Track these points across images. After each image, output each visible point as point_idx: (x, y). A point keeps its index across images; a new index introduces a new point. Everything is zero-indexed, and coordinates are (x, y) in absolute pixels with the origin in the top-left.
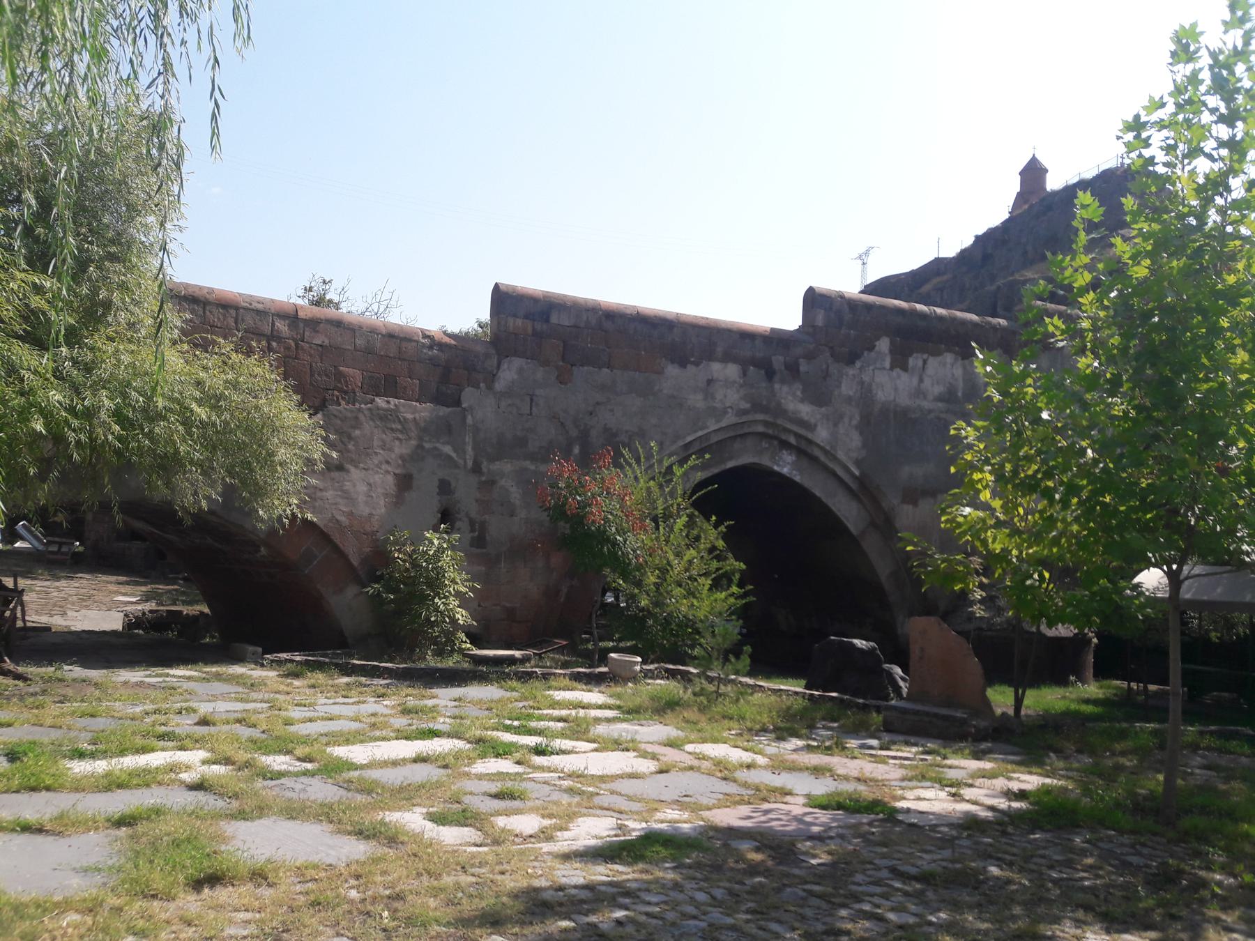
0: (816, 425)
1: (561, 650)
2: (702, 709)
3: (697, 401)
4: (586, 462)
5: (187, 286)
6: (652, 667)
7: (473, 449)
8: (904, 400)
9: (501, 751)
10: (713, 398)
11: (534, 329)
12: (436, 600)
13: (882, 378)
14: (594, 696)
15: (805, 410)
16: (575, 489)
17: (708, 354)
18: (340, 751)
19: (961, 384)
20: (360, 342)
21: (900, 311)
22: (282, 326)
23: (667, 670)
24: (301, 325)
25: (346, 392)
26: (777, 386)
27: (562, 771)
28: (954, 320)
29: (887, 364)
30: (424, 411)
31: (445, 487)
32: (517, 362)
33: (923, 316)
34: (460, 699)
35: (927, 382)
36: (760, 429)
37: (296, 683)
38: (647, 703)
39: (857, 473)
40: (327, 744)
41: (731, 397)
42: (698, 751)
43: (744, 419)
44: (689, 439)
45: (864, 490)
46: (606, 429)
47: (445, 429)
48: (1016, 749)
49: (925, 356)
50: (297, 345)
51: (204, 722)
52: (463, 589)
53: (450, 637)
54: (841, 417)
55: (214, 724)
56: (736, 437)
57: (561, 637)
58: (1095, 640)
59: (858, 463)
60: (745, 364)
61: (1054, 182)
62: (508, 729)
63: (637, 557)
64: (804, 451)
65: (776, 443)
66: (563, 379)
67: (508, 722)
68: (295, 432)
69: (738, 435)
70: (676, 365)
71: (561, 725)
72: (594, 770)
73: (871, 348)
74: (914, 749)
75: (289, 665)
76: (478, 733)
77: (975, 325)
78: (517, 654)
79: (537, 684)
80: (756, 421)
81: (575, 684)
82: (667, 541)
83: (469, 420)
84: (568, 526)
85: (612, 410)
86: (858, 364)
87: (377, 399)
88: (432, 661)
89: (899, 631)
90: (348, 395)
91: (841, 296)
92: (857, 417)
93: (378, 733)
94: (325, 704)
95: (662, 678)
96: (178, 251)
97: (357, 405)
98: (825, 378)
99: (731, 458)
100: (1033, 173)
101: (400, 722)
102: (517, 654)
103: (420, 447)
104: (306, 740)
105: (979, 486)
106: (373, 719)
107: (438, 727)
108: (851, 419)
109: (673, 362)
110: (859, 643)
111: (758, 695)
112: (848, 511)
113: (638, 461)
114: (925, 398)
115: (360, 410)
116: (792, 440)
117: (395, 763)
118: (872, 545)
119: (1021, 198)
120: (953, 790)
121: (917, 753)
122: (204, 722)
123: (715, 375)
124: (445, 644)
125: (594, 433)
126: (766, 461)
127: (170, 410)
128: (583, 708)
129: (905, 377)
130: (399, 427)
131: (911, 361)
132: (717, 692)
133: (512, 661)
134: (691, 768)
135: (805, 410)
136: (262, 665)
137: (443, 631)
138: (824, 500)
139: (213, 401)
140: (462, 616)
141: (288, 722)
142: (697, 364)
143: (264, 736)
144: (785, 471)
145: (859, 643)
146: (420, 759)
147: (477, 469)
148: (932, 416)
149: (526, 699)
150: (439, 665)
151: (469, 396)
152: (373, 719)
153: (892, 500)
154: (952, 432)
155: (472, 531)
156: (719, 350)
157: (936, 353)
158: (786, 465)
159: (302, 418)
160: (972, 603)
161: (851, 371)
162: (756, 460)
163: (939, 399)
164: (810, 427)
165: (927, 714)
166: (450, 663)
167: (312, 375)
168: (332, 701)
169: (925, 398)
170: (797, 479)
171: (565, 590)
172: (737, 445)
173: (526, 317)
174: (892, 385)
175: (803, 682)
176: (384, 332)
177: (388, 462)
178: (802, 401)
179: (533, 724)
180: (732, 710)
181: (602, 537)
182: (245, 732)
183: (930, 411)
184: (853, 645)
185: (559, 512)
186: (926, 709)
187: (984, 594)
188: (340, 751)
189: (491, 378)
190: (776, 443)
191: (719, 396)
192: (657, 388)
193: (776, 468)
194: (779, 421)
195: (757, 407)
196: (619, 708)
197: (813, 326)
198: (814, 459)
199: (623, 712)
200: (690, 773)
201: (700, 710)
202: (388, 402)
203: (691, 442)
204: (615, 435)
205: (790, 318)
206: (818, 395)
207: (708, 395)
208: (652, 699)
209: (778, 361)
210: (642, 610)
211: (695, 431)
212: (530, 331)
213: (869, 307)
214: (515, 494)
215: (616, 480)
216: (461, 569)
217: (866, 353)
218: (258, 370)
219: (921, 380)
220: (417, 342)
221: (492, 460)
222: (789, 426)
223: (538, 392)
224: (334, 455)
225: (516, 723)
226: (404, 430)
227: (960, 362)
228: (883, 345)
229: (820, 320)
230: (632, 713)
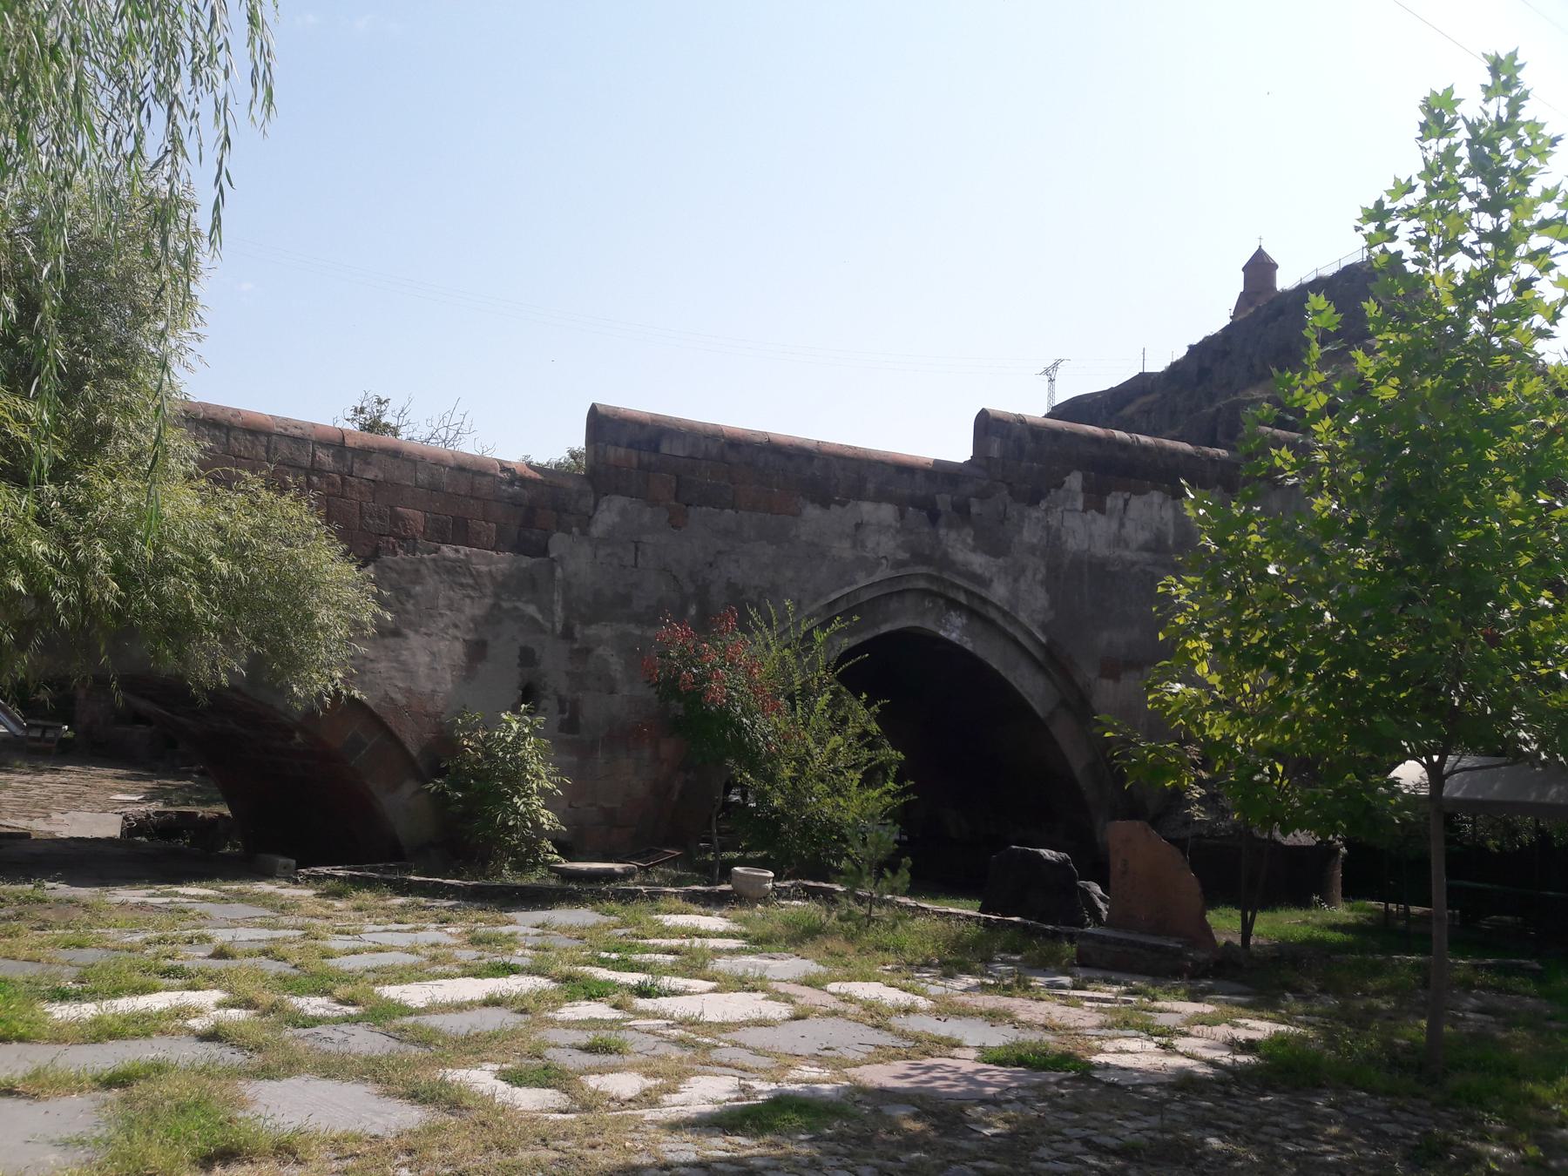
0: (991, 581)
1: (672, 863)
2: (850, 938)
3: (843, 549)
4: (705, 625)
5: (206, 406)
6: (787, 884)
7: (563, 608)
8: (1101, 550)
9: (596, 992)
10: (863, 546)
11: (639, 460)
12: (516, 800)
13: (1073, 522)
14: (713, 922)
15: (978, 562)
16: (691, 659)
17: (857, 491)
18: (392, 992)
19: (1171, 529)
20: (422, 477)
21: (1095, 440)
22: (324, 456)
23: (806, 888)
24: (349, 455)
25: (404, 539)
26: (942, 532)
27: (671, 1017)
28: (1162, 449)
30: (501, 562)
31: (527, 657)
32: (619, 501)
33: (1123, 445)
34: (544, 926)
35: (1129, 528)
36: (922, 584)
37: (338, 904)
38: (780, 930)
39: (1043, 640)
40: (375, 983)
41: (886, 545)
42: (843, 991)
43: (902, 572)
44: (834, 596)
45: (1052, 661)
47: (528, 584)
48: (1240, 987)
49: (1127, 495)
50: (343, 480)
51: (221, 954)
52: (549, 785)
53: (533, 847)
54: (1023, 570)
55: (233, 957)
56: (892, 594)
57: (673, 846)
58: (1343, 850)
59: (1044, 628)
60: (902, 504)
61: (1285, 280)
62: (604, 963)
63: (768, 744)
64: (977, 612)
65: (941, 602)
66: (676, 522)
67: (604, 955)
68: (339, 587)
69: (895, 592)
71: (671, 958)
72: (711, 1016)
73: (1060, 485)
74: (1115, 989)
75: (329, 882)
76: (566, 969)
77: (1188, 456)
78: (618, 867)
79: (642, 906)
80: (916, 575)
81: (691, 906)
82: (806, 724)
83: (559, 572)
84: (681, 705)
86: (1043, 505)
87: (444, 548)
88: (509, 877)
90: (408, 542)
91: (1021, 420)
92: (1043, 570)
93: (439, 969)
94: (373, 933)
95: (799, 899)
96: (195, 364)
97: (418, 555)
98: (1002, 522)
99: (885, 621)
100: (1259, 269)
101: (468, 955)
102: (618, 867)
103: (496, 606)
104: (349, 978)
105: (1195, 657)
106: (434, 951)
107: (515, 961)
109: (813, 501)
110: (1046, 853)
111: (919, 920)
112: (1032, 687)
113: (769, 625)
114: (1127, 546)
115: (421, 561)
116: (962, 598)
117: (460, 1007)
118: (1063, 732)
119: (1245, 299)
120: (1164, 1040)
121: (1119, 993)
122: (221, 954)
123: (866, 518)
124: (527, 855)
126: (929, 625)
127: (182, 562)
128: (700, 936)
129: (1102, 520)
130: (471, 581)
131: (1109, 502)
132: (868, 916)
133: (610, 876)
134: (835, 1013)
135: (978, 562)
136: (296, 882)
137: (523, 839)
139: (236, 551)
140: (547, 819)
141: (327, 955)
142: (842, 504)
143: (296, 972)
144: (954, 636)
145: (1046, 853)
146: (492, 1002)
147: (568, 634)
148: (1136, 569)
149: (627, 925)
150: (518, 882)
151: (559, 544)
152: (434, 951)
154: (1160, 590)
155: (562, 711)
156: (871, 487)
157: (1140, 492)
158: (954, 630)
159: (350, 571)
160: (1190, 803)
162: (917, 623)
163: (1145, 547)
164: (985, 583)
165: (1133, 943)
166: (532, 879)
167: (362, 518)
168: (382, 928)
169: (1127, 546)
170: (969, 647)
172: (894, 605)
173: (630, 446)
174: (1086, 531)
175: (978, 904)
176: (452, 463)
177: (456, 626)
178: (974, 550)
179: (636, 957)
180: (888, 939)
181: (724, 718)
182: (273, 967)
183: (1133, 564)
184: (1041, 856)
185: (669, 687)
186: (1131, 937)
187: (1203, 792)
188: (392, 992)
189: (586, 520)
191: (870, 545)
194: (945, 576)
195: (918, 557)
196: (745, 936)
197: (988, 458)
198: (989, 623)
199: (750, 942)
200: (831, 1020)
201: (846, 939)
202: (457, 551)
203: (836, 601)
205: (958, 449)
206: (994, 542)
207: (857, 543)
208: (787, 925)
209: (944, 501)
210: (775, 811)
212: (635, 461)
213: (1056, 434)
214: (616, 665)
215: (744, 649)
216: (545, 762)
218: (294, 512)
219: (1122, 525)
220: (494, 476)
221: (587, 622)
222: (959, 581)
224: (389, 616)
225: (614, 956)
226: (477, 586)
227: (1170, 502)
228: (1075, 481)
229: (995, 450)
230: (760, 943)
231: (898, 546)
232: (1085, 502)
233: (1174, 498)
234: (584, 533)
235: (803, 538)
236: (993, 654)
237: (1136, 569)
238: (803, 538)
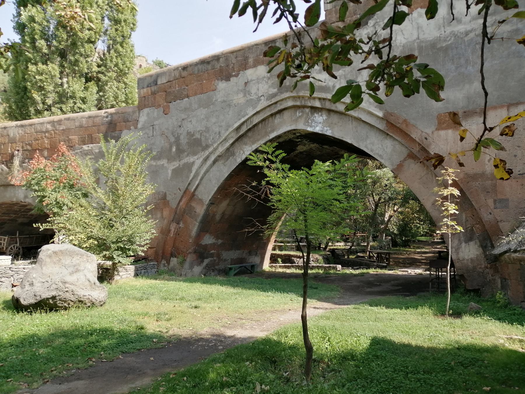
3: (239, 99)
10: (250, 93)
17: (244, 66)
32: (146, 111)
36: (290, 103)
39: (380, 114)
43: (274, 101)
44: (236, 125)
46: (188, 133)
56: (272, 115)
70: (224, 81)
80: (285, 99)
85: (191, 121)
99: (273, 131)
123: (250, 79)
125: (182, 137)
142: (237, 76)
144: (318, 129)
170: (329, 133)
171: (173, 230)
172: (278, 120)
173: (148, 86)
183: (467, 33)
190: (307, 110)
191: (253, 91)
192: (214, 100)
193: (310, 129)
202: (88, 147)
204: (193, 135)
211: (240, 119)
223: (155, 123)
231: (269, 87)
234: (136, 128)
235: (219, 100)
238: (219, 100)
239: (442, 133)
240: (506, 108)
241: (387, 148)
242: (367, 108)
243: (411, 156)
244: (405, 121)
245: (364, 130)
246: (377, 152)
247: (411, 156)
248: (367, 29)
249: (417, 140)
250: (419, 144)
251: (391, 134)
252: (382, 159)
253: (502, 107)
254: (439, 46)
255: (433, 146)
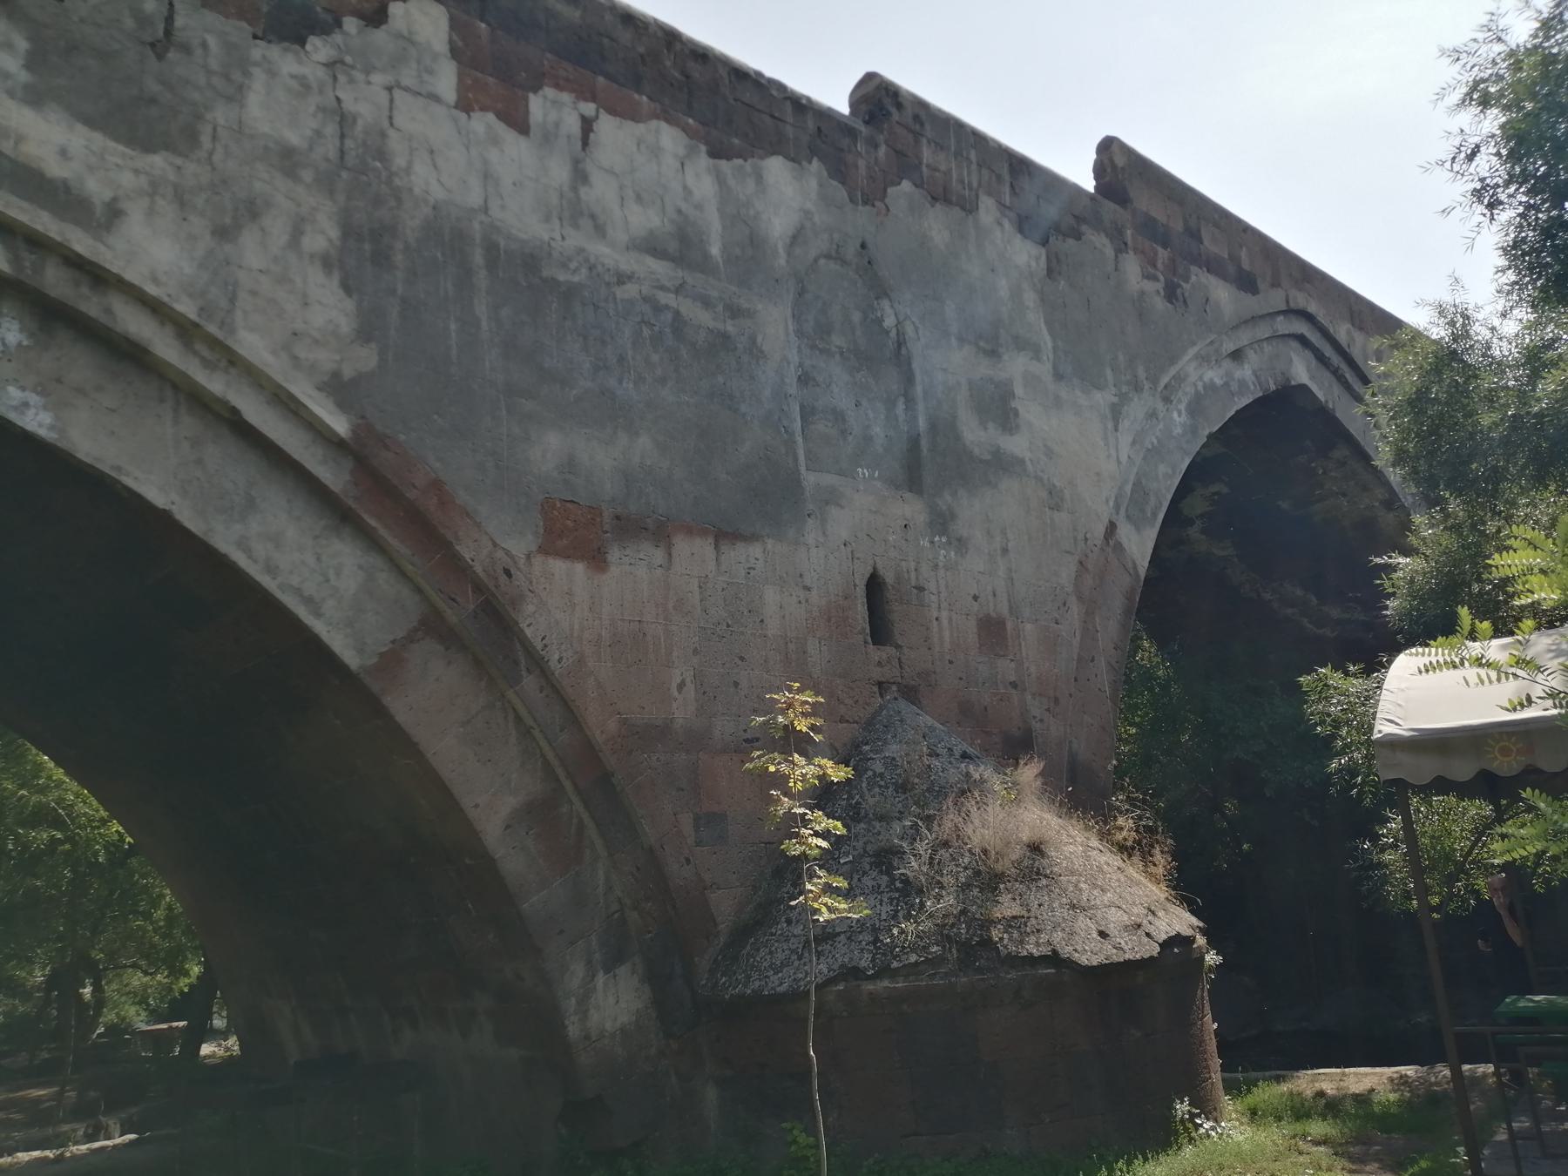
0: (114, 213)
8: (524, 221)
29: (446, 81)
35: (602, 191)
39: (340, 425)
45: (377, 496)
49: (589, 108)
54: (252, 210)
58: (1212, 958)
59: (339, 388)
86: (319, 49)
89: (573, 1030)
92: (334, 233)
108: (297, 234)
112: (323, 581)
114: (600, 230)
118: (436, 709)
131: (538, 106)
138: (186, 516)
148: (630, 291)
153: (499, 537)
161: (287, 62)
163: (650, 246)
198: (130, 356)
217: (351, 24)
219: (580, 176)
227: (703, 161)
232: (462, 88)
233: (715, 154)
236: (151, 461)
237: (630, 291)
239: (558, 566)
240: (711, 540)
241: (338, 574)
242: (279, 379)
243: (432, 626)
244: (437, 485)
245: (230, 467)
246: (295, 581)
247: (432, 626)
248: (300, 62)
249: (479, 569)
250: (479, 588)
251: (373, 522)
252: (318, 615)
253: (703, 533)
254: (546, 273)
255: (531, 608)
